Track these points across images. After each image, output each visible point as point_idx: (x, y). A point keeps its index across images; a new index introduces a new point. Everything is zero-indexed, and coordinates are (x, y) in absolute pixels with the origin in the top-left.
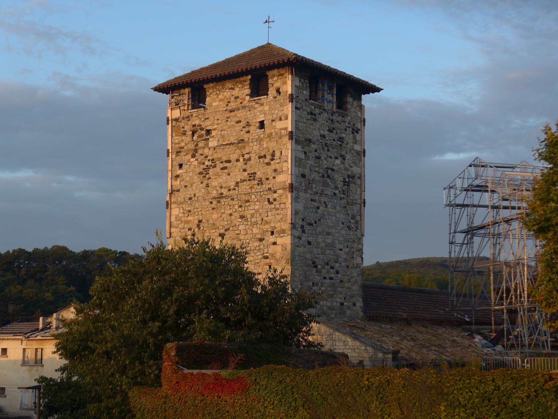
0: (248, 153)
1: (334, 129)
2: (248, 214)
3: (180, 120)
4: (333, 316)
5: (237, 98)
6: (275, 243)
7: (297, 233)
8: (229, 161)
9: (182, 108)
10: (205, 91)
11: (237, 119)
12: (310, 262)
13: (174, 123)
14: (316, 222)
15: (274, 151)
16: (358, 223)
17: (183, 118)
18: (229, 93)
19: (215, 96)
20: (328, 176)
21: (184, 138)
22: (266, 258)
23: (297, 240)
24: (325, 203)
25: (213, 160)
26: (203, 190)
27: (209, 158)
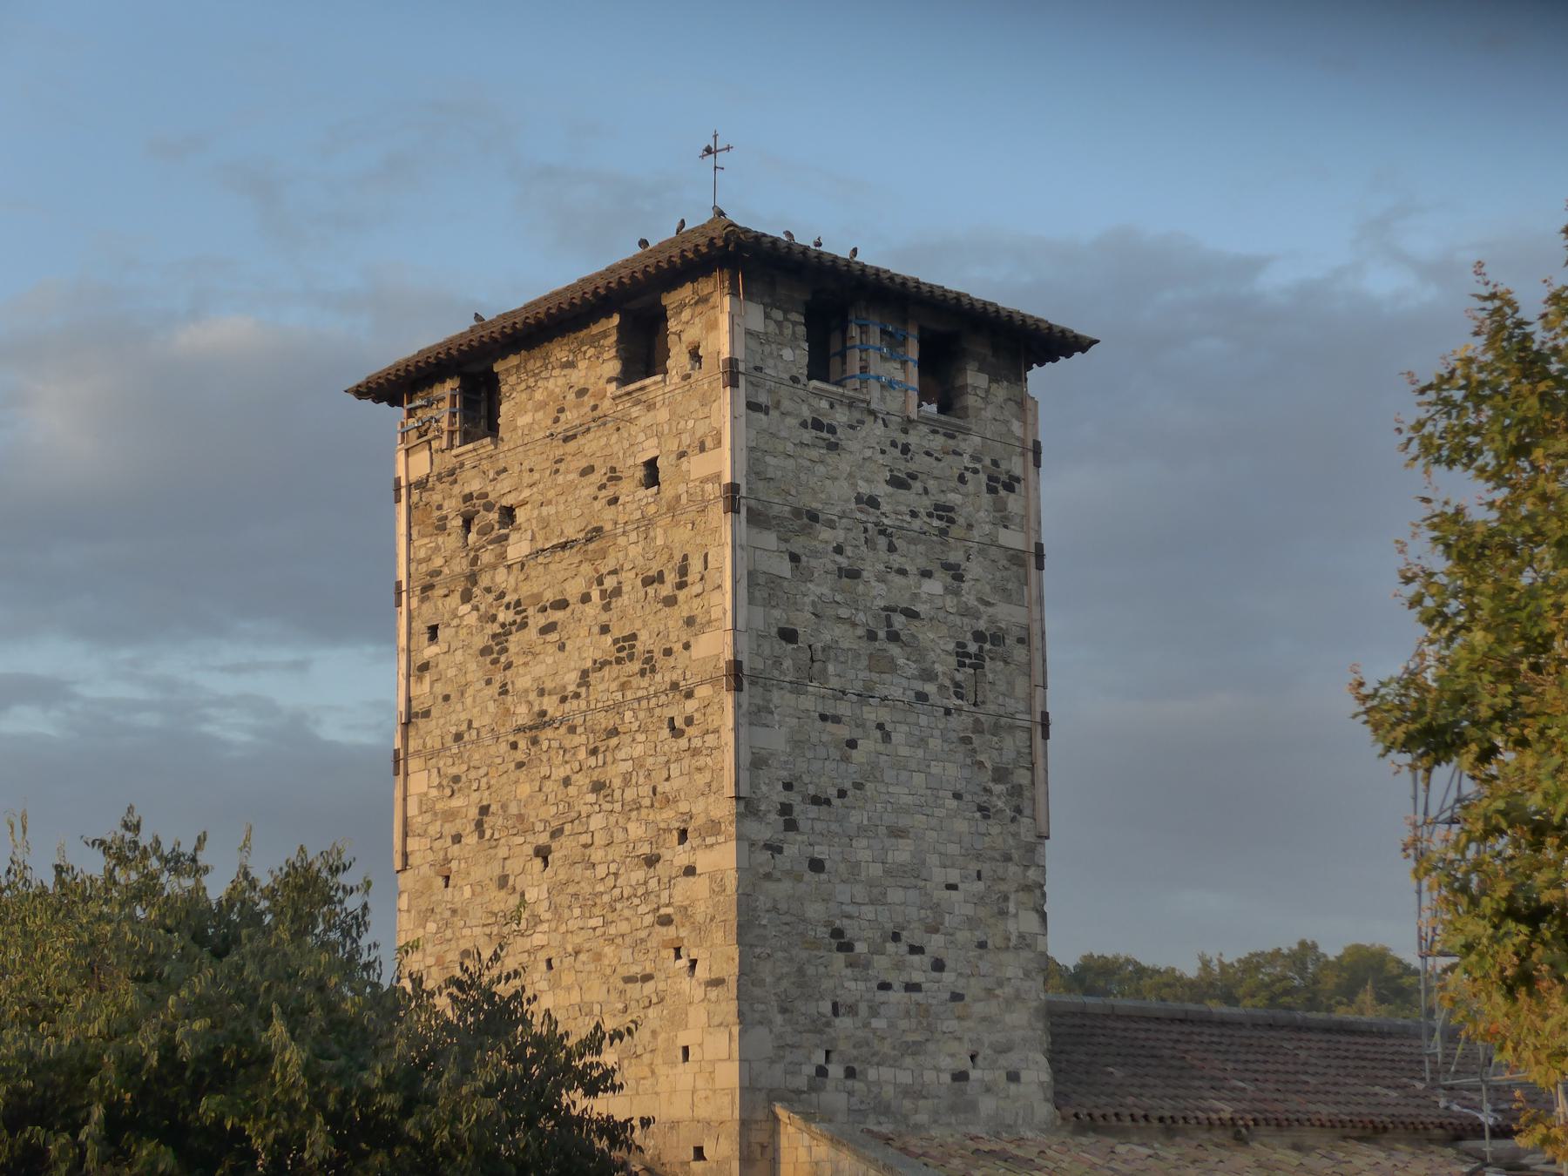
0: (614, 572)
1: (913, 477)
2: (614, 774)
3: (430, 485)
4: (922, 1118)
5: (582, 392)
6: (690, 871)
8: (562, 604)
9: (435, 444)
10: (498, 382)
11: (584, 464)
12: (823, 932)
13: (416, 494)
14: (842, 794)
15: (685, 558)
16: (1020, 795)
17: (440, 478)
18: (561, 381)
19: (524, 396)
20: (894, 637)
21: (440, 540)
22: (666, 921)
24: (880, 726)
25: (518, 603)
26: (492, 707)
27: (506, 600)
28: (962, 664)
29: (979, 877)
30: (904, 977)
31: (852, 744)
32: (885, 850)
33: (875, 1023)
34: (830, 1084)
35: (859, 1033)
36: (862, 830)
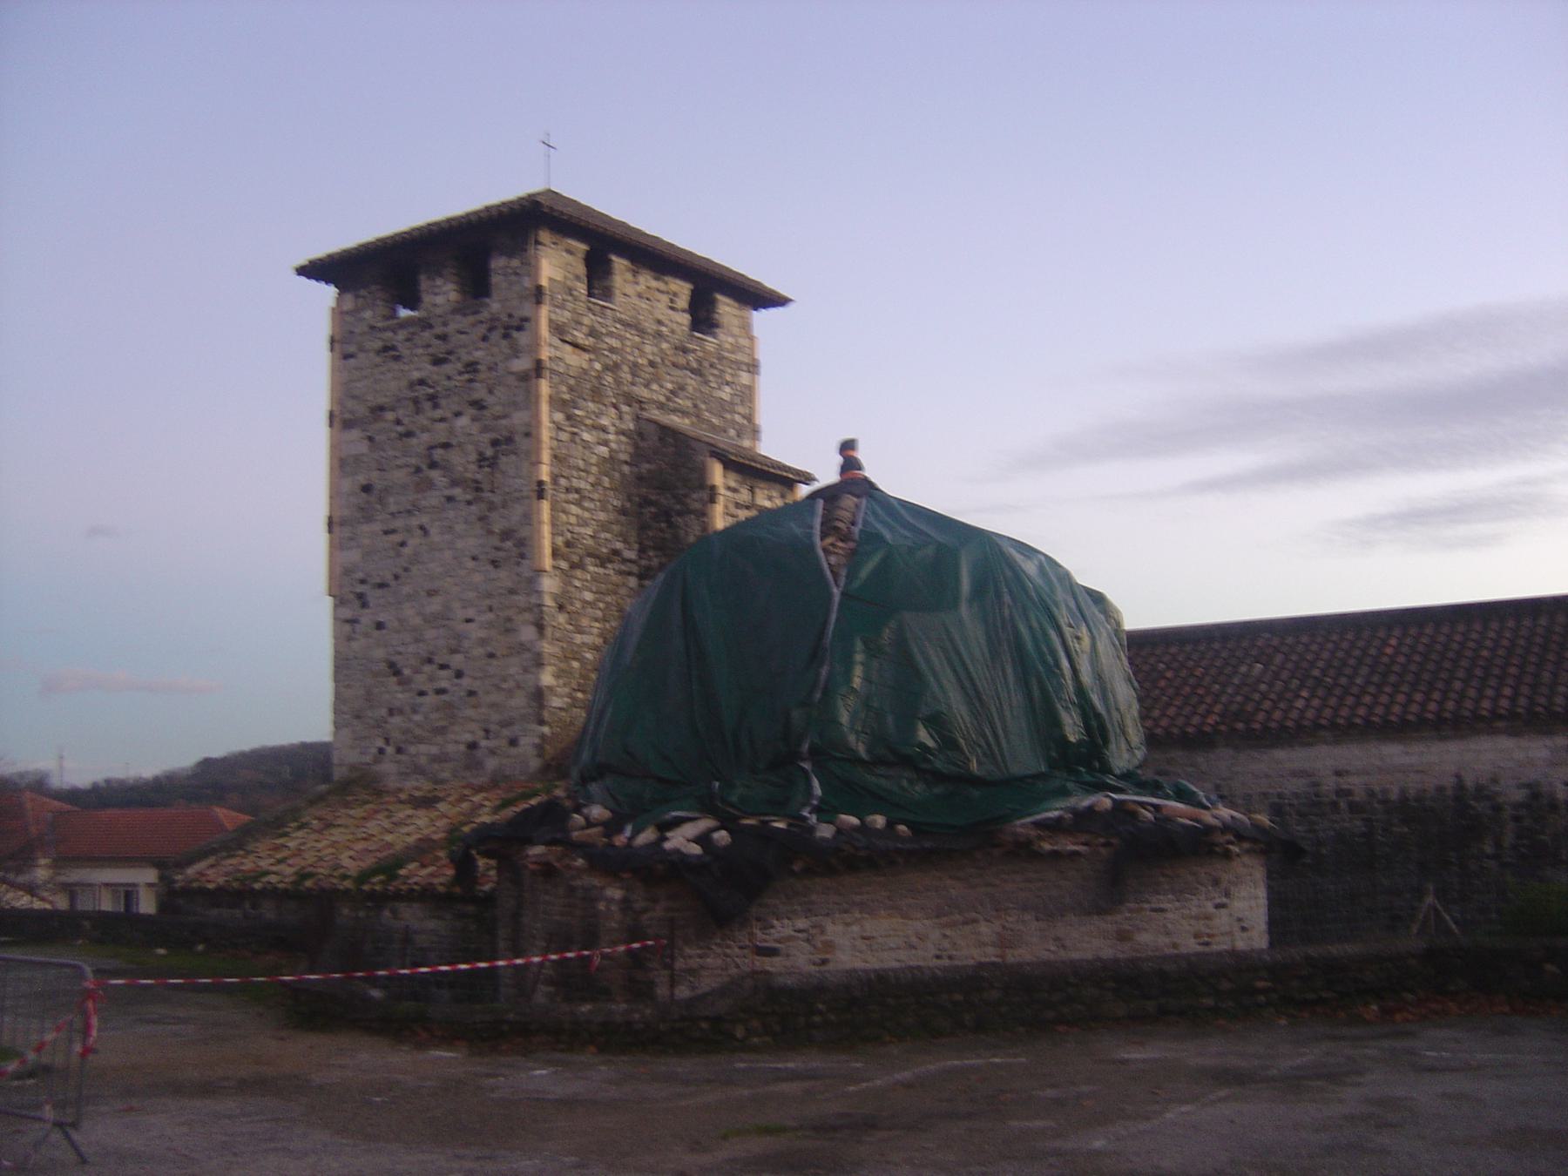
1: (450, 353)
4: (446, 775)
7: (347, 613)
12: (383, 666)
14: (396, 577)
20: (433, 465)
23: (347, 627)
24: (422, 528)
31: (403, 544)
36: (409, 597)
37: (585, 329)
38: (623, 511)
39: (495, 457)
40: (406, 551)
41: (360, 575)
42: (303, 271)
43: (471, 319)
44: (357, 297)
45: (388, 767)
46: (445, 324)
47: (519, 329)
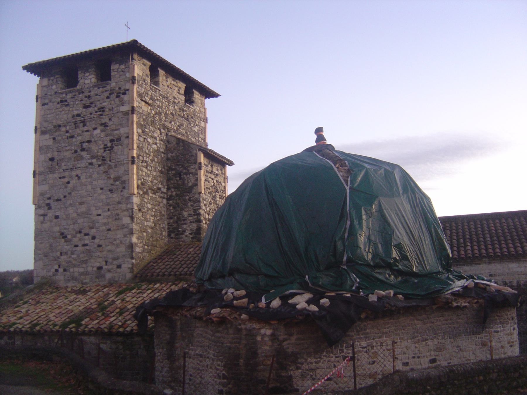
1: (92, 103)
4: (87, 281)
7: (42, 212)
12: (58, 234)
14: (65, 197)
16: (125, 183)
20: (83, 150)
23: (42, 218)
28: (105, 151)
29: (109, 210)
30: (83, 242)
32: (77, 209)
33: (73, 256)
34: (59, 273)
35: (69, 259)
36: (71, 205)
37: (149, 97)
38: (161, 172)
39: (112, 146)
40: (69, 185)
41: (48, 196)
42: (26, 68)
43: (101, 90)
44: (49, 80)
45: (60, 278)
46: (90, 92)
47: (124, 94)
